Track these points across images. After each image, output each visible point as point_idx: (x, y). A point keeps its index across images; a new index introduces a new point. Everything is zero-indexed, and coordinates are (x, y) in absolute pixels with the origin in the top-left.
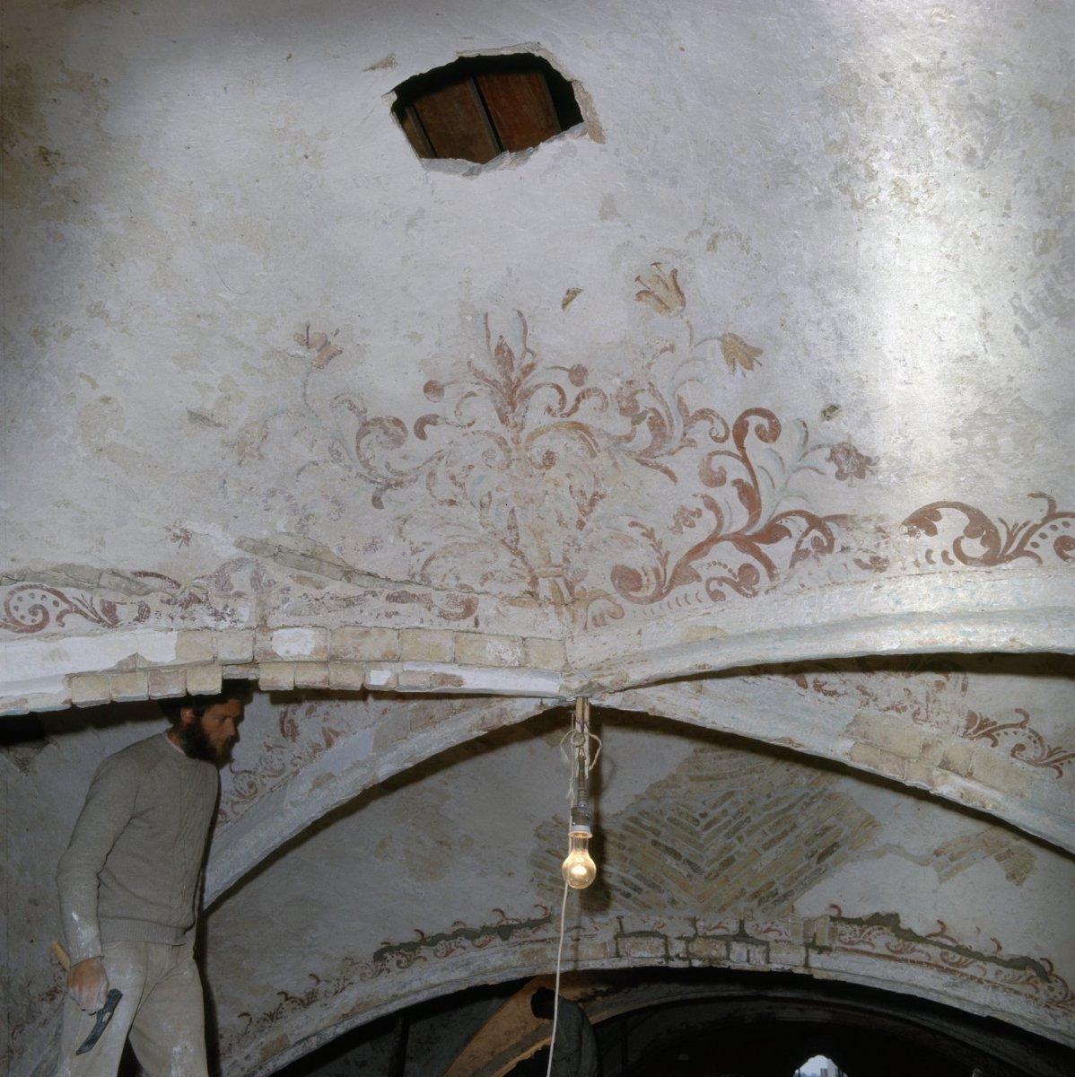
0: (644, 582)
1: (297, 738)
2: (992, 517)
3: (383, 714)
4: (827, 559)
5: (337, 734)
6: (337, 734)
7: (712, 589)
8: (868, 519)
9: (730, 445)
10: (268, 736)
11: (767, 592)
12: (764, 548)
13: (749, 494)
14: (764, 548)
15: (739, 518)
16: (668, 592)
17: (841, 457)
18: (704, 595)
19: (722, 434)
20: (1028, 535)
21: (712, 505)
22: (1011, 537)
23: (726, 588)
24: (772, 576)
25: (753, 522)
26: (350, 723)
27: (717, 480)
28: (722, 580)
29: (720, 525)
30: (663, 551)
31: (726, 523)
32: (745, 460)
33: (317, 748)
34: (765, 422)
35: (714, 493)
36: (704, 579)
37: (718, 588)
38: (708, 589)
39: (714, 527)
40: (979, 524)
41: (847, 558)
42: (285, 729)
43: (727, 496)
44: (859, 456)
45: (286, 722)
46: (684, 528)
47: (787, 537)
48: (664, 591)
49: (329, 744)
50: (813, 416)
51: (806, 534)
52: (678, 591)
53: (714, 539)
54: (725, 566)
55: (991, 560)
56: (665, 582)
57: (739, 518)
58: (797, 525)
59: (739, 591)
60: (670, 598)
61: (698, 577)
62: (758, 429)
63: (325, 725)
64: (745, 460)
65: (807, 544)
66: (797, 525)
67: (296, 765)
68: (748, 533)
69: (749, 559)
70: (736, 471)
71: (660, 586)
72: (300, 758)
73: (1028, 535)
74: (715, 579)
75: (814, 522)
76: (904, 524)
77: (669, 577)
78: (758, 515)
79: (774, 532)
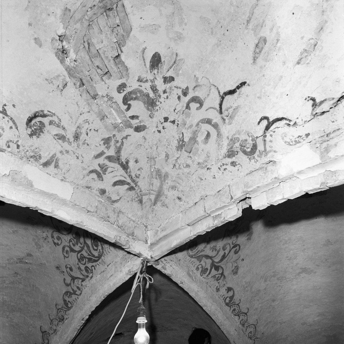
0: (194, 251)
1: (34, 137)
2: (234, 298)
3: (87, 187)
4: (216, 282)
5: (56, 166)
6: (56, 166)
7: (199, 267)
8: (226, 281)
9: (232, 246)
10: (14, 106)
11: (203, 278)
12: (213, 269)
13: (224, 257)
14: (213, 269)
15: (217, 260)
16: (194, 258)
17: (236, 268)
18: (196, 266)
19: (233, 243)
20: (233, 305)
21: (218, 252)
22: (232, 303)
23: (200, 269)
24: (207, 276)
25: (218, 263)
26: (71, 172)
27: (224, 249)
28: (202, 267)
29: (215, 257)
30: (204, 249)
31: (215, 258)
32: (230, 251)
33: (36, 157)
34: (238, 249)
35: (221, 249)
36: (201, 263)
37: (200, 268)
38: (198, 266)
39: (214, 256)
40: (232, 298)
41: (217, 285)
42: (33, 122)
43: (221, 253)
44: (237, 271)
45: (39, 119)
46: (211, 250)
47: (217, 271)
48: (194, 257)
49: (46, 164)
50: (241, 258)
51: (219, 274)
52: (195, 260)
53: (211, 258)
54: (206, 265)
55: (227, 304)
56: (197, 255)
57: (217, 260)
58: (220, 271)
59: (201, 272)
60: (193, 259)
61: (200, 261)
62: (236, 249)
63: (59, 155)
64: (230, 251)
65: (217, 276)
66: (220, 271)
67: (9, 147)
68: (215, 264)
69: (209, 268)
70: (227, 252)
71: (195, 255)
72: (18, 147)
73: (233, 305)
74: (202, 265)
75: (222, 274)
76: (227, 287)
77: (198, 255)
78: (220, 263)
79: (217, 268)
